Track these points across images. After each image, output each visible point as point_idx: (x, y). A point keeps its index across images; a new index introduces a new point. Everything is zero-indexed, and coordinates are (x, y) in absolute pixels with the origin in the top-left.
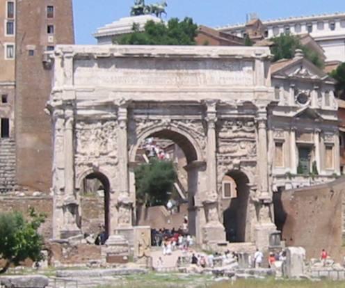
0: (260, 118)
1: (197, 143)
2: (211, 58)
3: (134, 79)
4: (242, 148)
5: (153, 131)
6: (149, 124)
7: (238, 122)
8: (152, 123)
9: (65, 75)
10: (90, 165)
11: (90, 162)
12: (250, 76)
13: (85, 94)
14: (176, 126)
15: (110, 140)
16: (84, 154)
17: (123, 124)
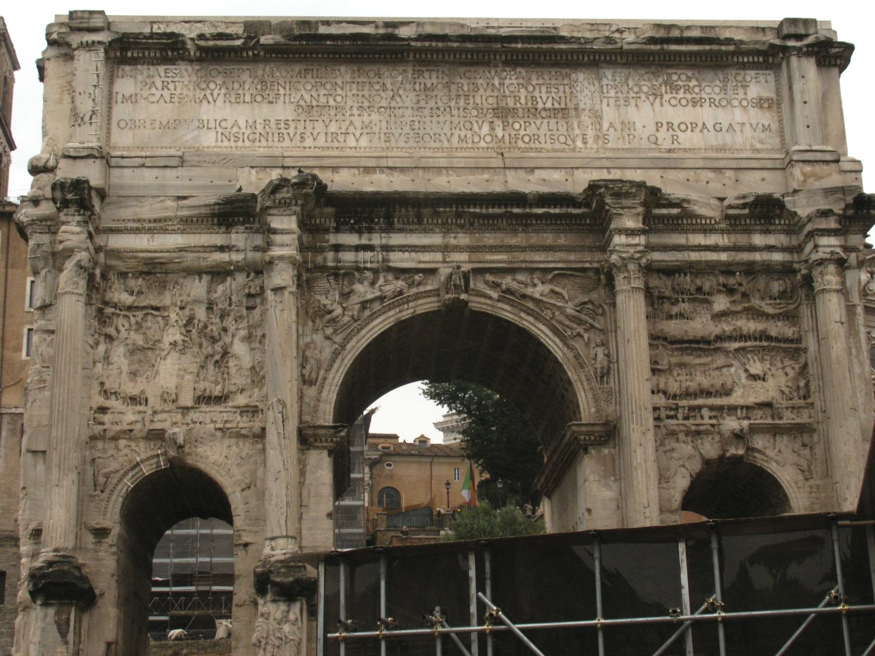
0: (821, 254)
1: (577, 357)
2: (621, 52)
3: (333, 128)
4: (754, 377)
5: (406, 313)
6: (391, 285)
7: (731, 281)
8: (400, 284)
9: (76, 115)
10: (156, 436)
11: (158, 426)
12: (766, 118)
13: (148, 176)
14: (495, 295)
15: (239, 348)
16: (134, 400)
17: (283, 276)
